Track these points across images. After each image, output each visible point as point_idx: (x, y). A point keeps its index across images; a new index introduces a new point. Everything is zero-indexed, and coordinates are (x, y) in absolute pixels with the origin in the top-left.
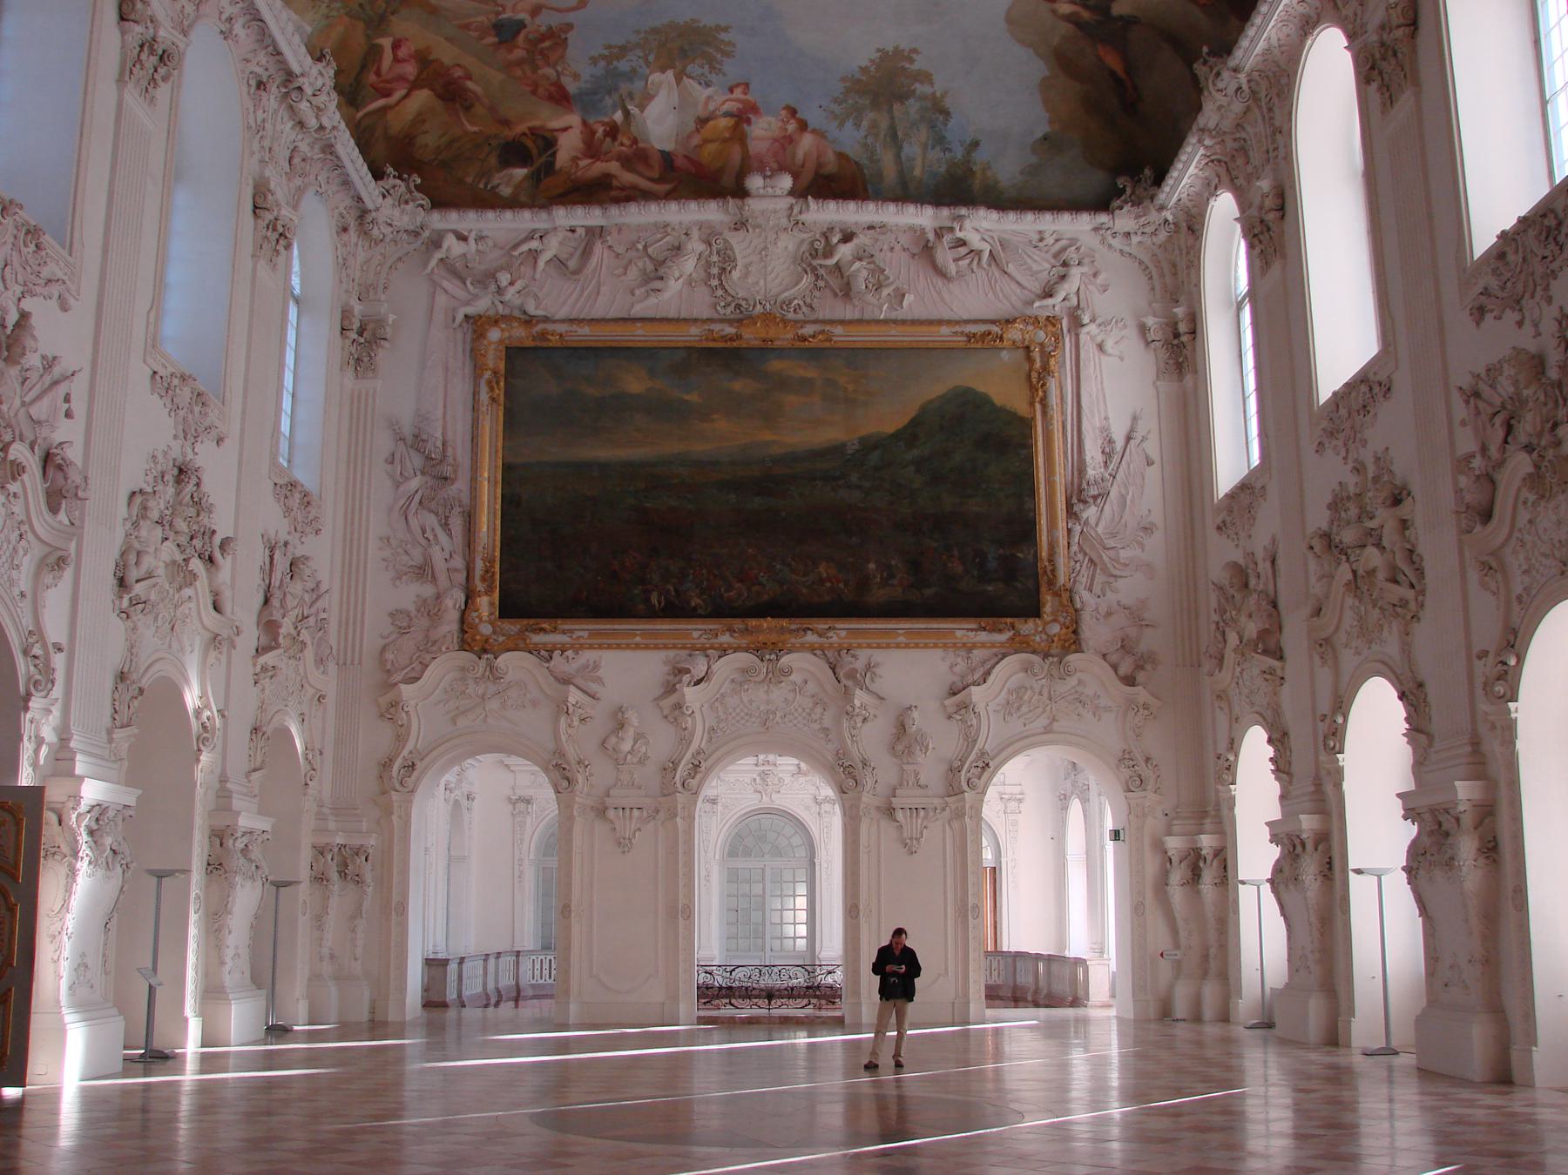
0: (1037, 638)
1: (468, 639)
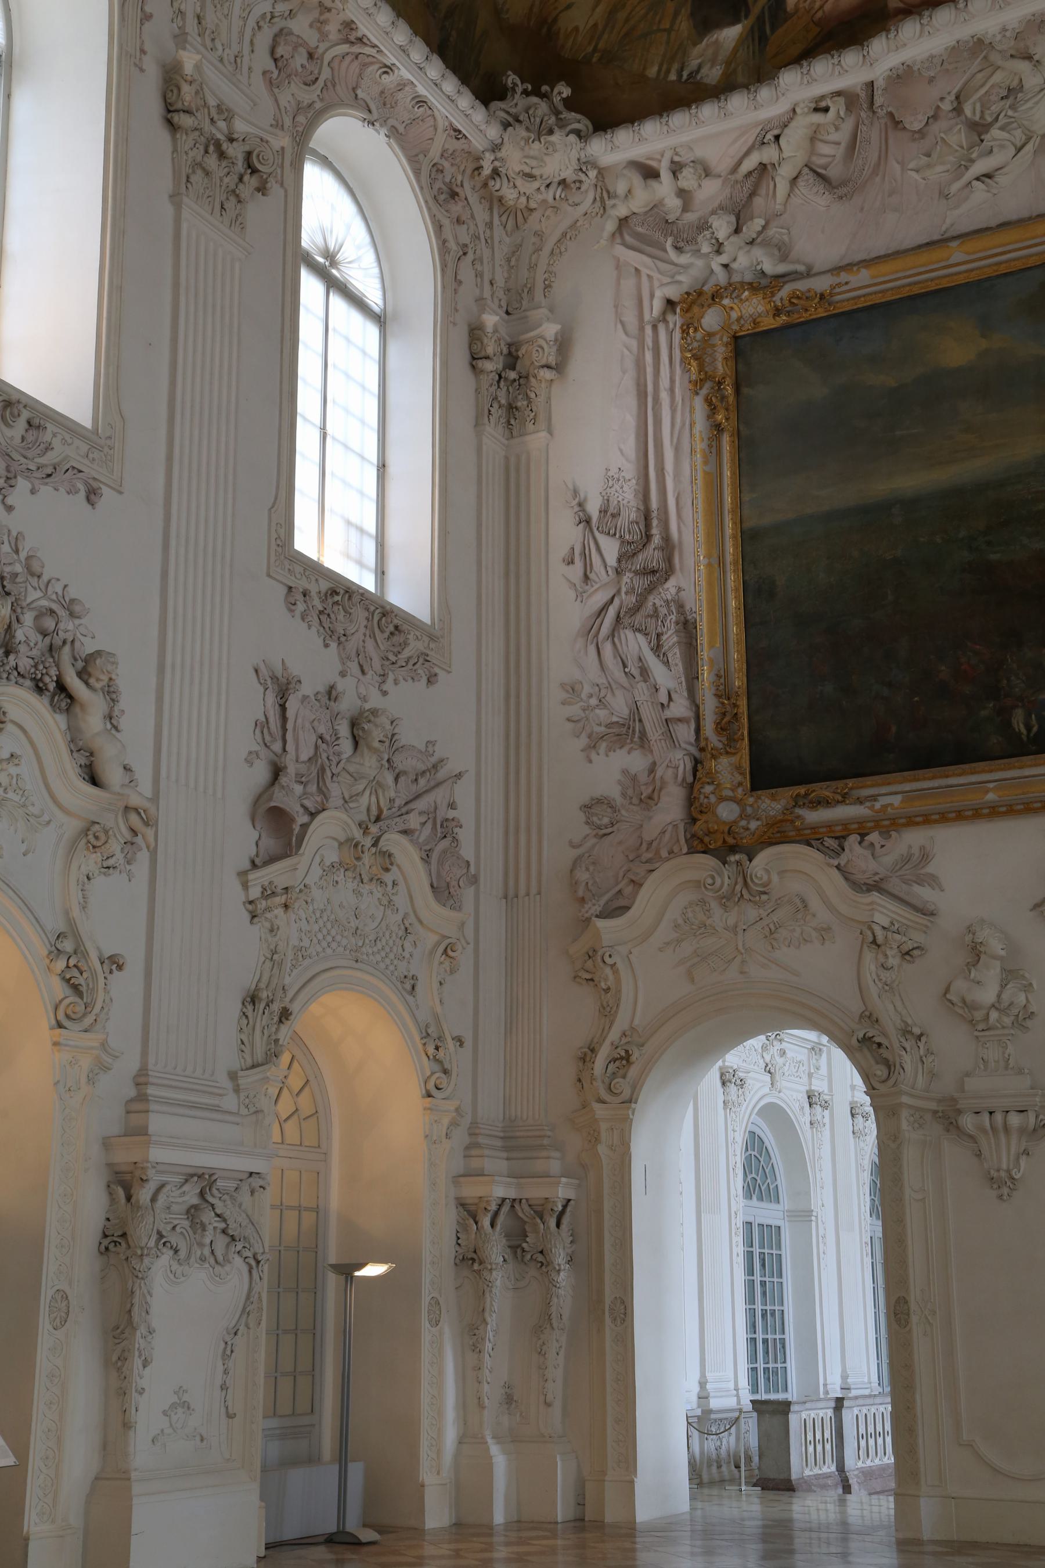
1: (709, 839)
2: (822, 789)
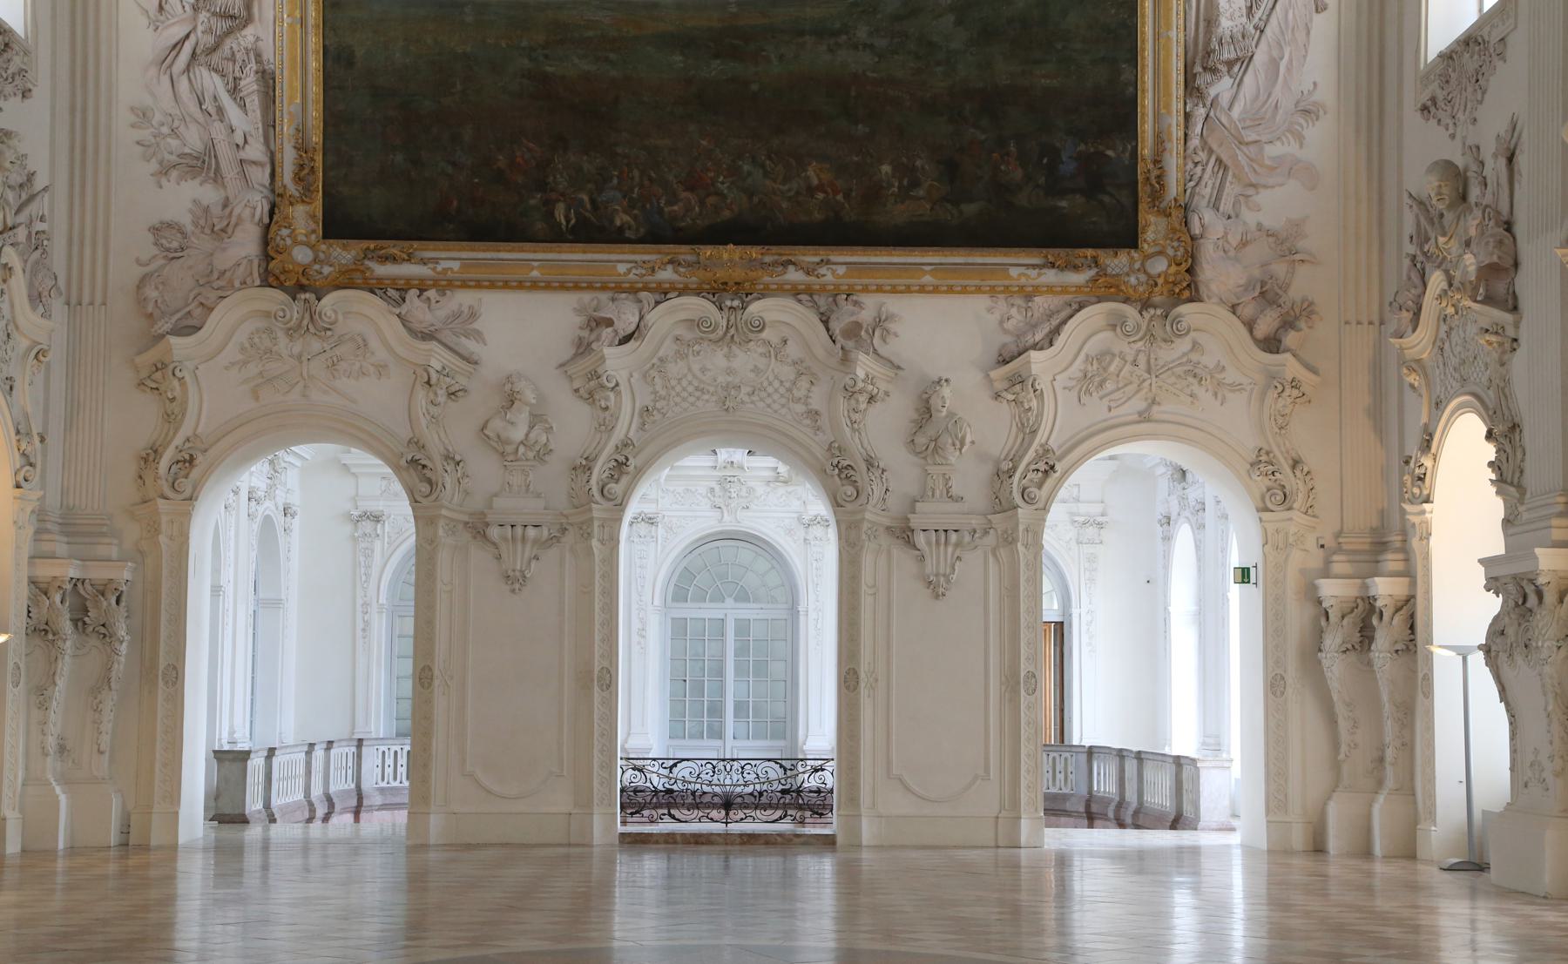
0: (1133, 280)
1: (273, 271)
2: (393, 247)
